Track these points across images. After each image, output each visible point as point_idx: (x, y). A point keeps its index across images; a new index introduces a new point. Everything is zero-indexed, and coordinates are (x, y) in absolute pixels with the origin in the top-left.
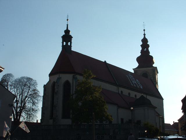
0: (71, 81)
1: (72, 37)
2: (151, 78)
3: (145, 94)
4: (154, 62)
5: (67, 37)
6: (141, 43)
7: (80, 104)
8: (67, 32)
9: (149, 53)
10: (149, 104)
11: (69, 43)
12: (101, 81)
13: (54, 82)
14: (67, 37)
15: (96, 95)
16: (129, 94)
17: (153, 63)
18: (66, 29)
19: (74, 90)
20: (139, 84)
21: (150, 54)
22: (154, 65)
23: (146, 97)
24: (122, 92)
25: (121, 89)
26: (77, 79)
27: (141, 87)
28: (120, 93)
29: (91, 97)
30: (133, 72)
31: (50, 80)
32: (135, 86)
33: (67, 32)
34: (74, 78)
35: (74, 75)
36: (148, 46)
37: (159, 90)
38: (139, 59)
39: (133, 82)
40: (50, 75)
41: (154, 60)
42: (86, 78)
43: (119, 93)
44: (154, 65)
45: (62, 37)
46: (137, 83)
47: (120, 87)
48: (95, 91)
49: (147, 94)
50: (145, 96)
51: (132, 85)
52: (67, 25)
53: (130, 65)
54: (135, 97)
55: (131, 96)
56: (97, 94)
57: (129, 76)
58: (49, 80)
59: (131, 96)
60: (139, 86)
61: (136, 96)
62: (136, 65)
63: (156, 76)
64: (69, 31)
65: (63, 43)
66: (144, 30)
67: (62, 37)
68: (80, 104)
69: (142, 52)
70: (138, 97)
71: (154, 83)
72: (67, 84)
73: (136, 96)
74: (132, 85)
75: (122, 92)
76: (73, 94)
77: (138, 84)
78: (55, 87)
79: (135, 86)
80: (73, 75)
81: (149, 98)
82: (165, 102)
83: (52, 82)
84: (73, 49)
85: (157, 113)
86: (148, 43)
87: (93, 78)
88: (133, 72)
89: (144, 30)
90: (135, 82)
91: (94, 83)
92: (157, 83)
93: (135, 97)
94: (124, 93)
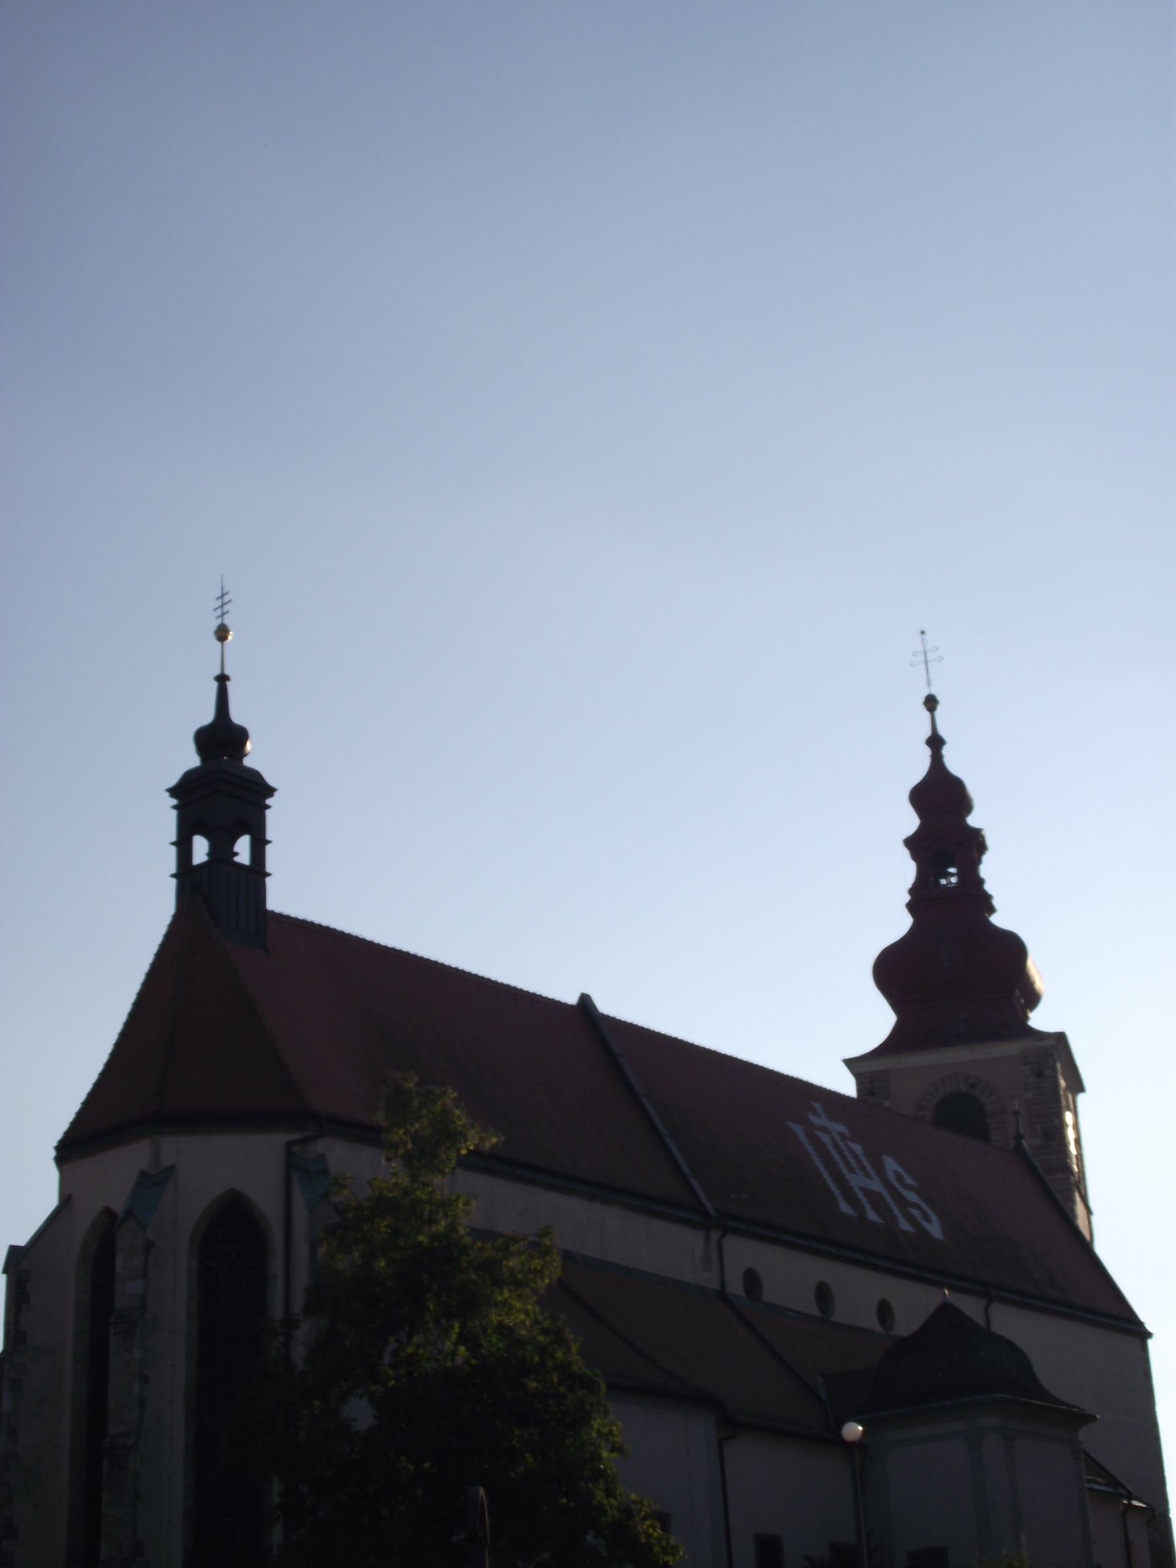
0: (267, 1201)
1: (270, 791)
2: (1019, 1137)
3: (966, 1291)
4: (1040, 983)
5: (222, 792)
6: (911, 822)
7: (360, 1413)
8: (221, 739)
9: (985, 904)
10: (1009, 1383)
11: (243, 849)
12: (549, 1187)
13: (108, 1213)
14: (222, 792)
15: (509, 1321)
16: (823, 1294)
17: (1032, 998)
18: (207, 716)
19: (302, 1280)
20: (911, 1196)
21: (996, 920)
22: (1040, 1019)
23: (979, 1319)
24: (751, 1279)
25: (743, 1253)
26: (325, 1172)
27: (935, 1229)
28: (736, 1288)
29: (462, 1339)
30: (846, 1085)
31: (66, 1200)
32: (872, 1216)
33: (221, 739)
34: (295, 1165)
35: (296, 1136)
36: (975, 844)
37: (1104, 1249)
38: (894, 971)
39: (856, 1181)
40: (70, 1150)
41: (1038, 968)
42: (408, 1159)
43: (722, 1295)
44: (1040, 1019)
45: (173, 792)
47: (738, 1232)
48: (499, 1283)
49: (988, 1292)
50: (971, 1307)
51: (845, 1208)
52: (222, 679)
53: (814, 1020)
55: (838, 1317)
56: (518, 1312)
57: (810, 1128)
58: (49, 1200)
59: (838, 1317)
61: (884, 1311)
62: (876, 1021)
63: (1068, 1117)
64: (241, 735)
65: (183, 846)
66: (931, 703)
67: (173, 792)
68: (360, 1413)
69: (921, 899)
70: (907, 1323)
71: (1054, 1182)
72: (232, 1228)
73: (884, 1311)
74: (845, 1208)
75: (751, 1279)
76: (290, 1323)
77: (903, 1203)
78: (120, 1262)
79: (872, 1216)
80: (289, 1144)
81: (1010, 1323)
82: (1161, 1356)
83: (87, 1215)
84: (284, 896)
85: (1095, 1467)
86: (973, 820)
87: (479, 1162)
88: (846, 1085)
89: (931, 703)
90: (871, 1181)
91: (482, 1205)
92: (1079, 1184)
93: (878, 1328)
94: (771, 1293)
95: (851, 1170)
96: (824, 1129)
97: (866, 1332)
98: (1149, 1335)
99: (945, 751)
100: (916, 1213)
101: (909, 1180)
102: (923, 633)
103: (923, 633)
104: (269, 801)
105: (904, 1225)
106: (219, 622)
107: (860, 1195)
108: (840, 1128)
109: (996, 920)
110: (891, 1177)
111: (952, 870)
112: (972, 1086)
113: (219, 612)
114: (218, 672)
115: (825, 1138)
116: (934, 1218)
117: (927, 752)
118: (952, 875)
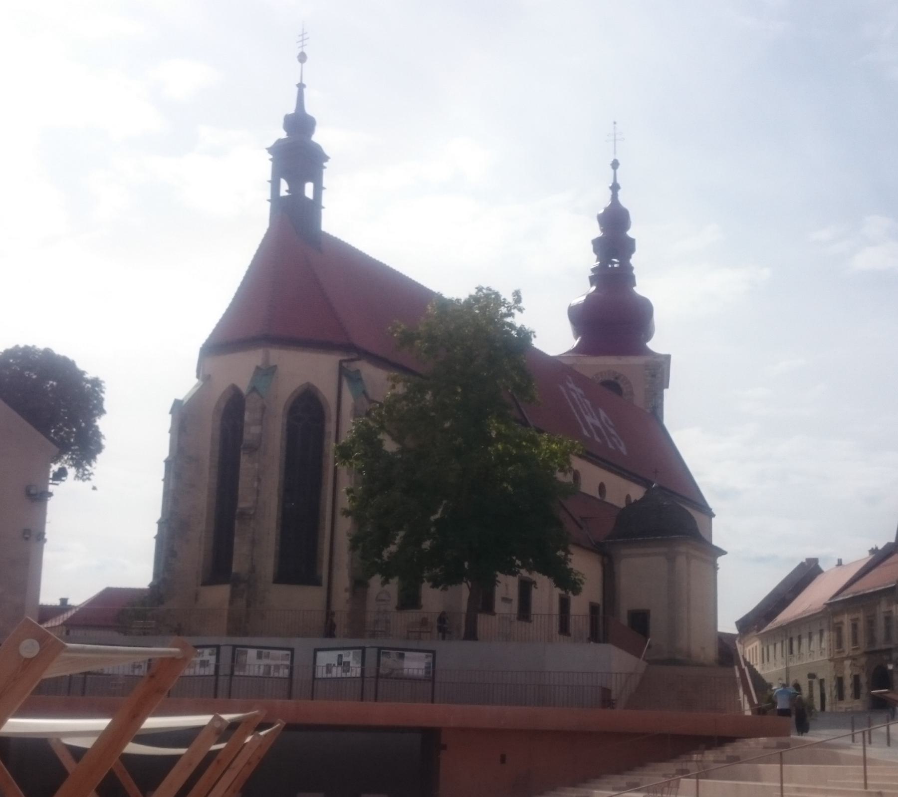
1: (326, 158)
5: (298, 157)
8: (299, 125)
14: (298, 157)
18: (291, 110)
20: (613, 432)
27: (623, 449)
32: (598, 439)
33: (299, 125)
35: (346, 358)
39: (588, 419)
46: (604, 427)
52: (301, 86)
54: (600, 494)
60: (615, 445)
79: (598, 439)
80: (341, 362)
83: (221, 387)
93: (598, 496)
95: (586, 414)
96: (572, 390)
97: (594, 498)
98: (714, 515)
99: (620, 192)
100: (615, 440)
101: (610, 423)
102: (615, 123)
103: (615, 123)
104: (325, 164)
105: (611, 446)
106: (300, 50)
107: (591, 427)
108: (579, 391)
109: (635, 289)
110: (603, 419)
111: (615, 260)
112: (616, 378)
113: (300, 44)
114: (298, 81)
115: (574, 396)
116: (622, 443)
117: (610, 193)
118: (615, 263)
